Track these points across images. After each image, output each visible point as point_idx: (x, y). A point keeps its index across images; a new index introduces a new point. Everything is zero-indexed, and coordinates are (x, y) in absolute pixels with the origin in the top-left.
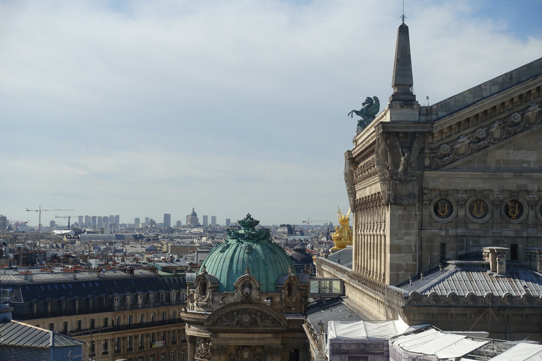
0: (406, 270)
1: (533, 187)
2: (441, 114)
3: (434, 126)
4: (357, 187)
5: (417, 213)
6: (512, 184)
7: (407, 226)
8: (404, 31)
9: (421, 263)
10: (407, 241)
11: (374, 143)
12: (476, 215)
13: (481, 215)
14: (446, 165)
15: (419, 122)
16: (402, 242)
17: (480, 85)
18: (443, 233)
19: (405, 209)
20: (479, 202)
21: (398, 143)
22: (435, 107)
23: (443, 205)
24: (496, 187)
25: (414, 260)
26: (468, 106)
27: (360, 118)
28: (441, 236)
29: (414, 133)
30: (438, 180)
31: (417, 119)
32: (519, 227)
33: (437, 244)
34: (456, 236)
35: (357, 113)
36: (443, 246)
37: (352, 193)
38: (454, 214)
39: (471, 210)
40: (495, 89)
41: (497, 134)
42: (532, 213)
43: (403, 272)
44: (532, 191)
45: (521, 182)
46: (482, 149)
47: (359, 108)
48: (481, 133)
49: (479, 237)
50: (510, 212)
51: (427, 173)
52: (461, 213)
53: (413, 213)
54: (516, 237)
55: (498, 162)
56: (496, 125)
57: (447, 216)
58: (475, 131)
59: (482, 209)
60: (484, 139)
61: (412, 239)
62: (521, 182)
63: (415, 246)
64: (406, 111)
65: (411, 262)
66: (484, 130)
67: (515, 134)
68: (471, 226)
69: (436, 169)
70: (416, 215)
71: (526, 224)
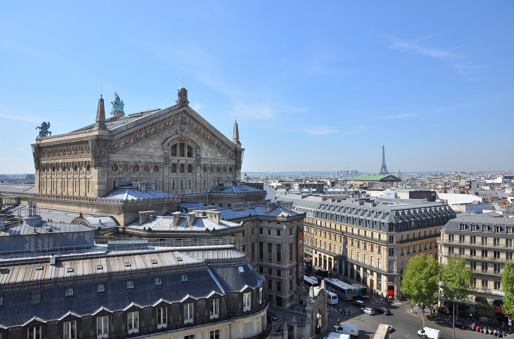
1: (143, 160)
4: (41, 159)
6: (137, 159)
7: (104, 175)
16: (102, 181)
20: (126, 166)
23: (115, 167)
24: (132, 160)
26: (124, 131)
30: (114, 157)
33: (113, 181)
35: (39, 128)
40: (132, 126)
42: (142, 170)
45: (139, 159)
47: (40, 126)
48: (128, 141)
51: (111, 155)
52: (121, 169)
57: (116, 170)
61: (105, 179)
62: (139, 159)
68: (123, 174)
71: (140, 174)
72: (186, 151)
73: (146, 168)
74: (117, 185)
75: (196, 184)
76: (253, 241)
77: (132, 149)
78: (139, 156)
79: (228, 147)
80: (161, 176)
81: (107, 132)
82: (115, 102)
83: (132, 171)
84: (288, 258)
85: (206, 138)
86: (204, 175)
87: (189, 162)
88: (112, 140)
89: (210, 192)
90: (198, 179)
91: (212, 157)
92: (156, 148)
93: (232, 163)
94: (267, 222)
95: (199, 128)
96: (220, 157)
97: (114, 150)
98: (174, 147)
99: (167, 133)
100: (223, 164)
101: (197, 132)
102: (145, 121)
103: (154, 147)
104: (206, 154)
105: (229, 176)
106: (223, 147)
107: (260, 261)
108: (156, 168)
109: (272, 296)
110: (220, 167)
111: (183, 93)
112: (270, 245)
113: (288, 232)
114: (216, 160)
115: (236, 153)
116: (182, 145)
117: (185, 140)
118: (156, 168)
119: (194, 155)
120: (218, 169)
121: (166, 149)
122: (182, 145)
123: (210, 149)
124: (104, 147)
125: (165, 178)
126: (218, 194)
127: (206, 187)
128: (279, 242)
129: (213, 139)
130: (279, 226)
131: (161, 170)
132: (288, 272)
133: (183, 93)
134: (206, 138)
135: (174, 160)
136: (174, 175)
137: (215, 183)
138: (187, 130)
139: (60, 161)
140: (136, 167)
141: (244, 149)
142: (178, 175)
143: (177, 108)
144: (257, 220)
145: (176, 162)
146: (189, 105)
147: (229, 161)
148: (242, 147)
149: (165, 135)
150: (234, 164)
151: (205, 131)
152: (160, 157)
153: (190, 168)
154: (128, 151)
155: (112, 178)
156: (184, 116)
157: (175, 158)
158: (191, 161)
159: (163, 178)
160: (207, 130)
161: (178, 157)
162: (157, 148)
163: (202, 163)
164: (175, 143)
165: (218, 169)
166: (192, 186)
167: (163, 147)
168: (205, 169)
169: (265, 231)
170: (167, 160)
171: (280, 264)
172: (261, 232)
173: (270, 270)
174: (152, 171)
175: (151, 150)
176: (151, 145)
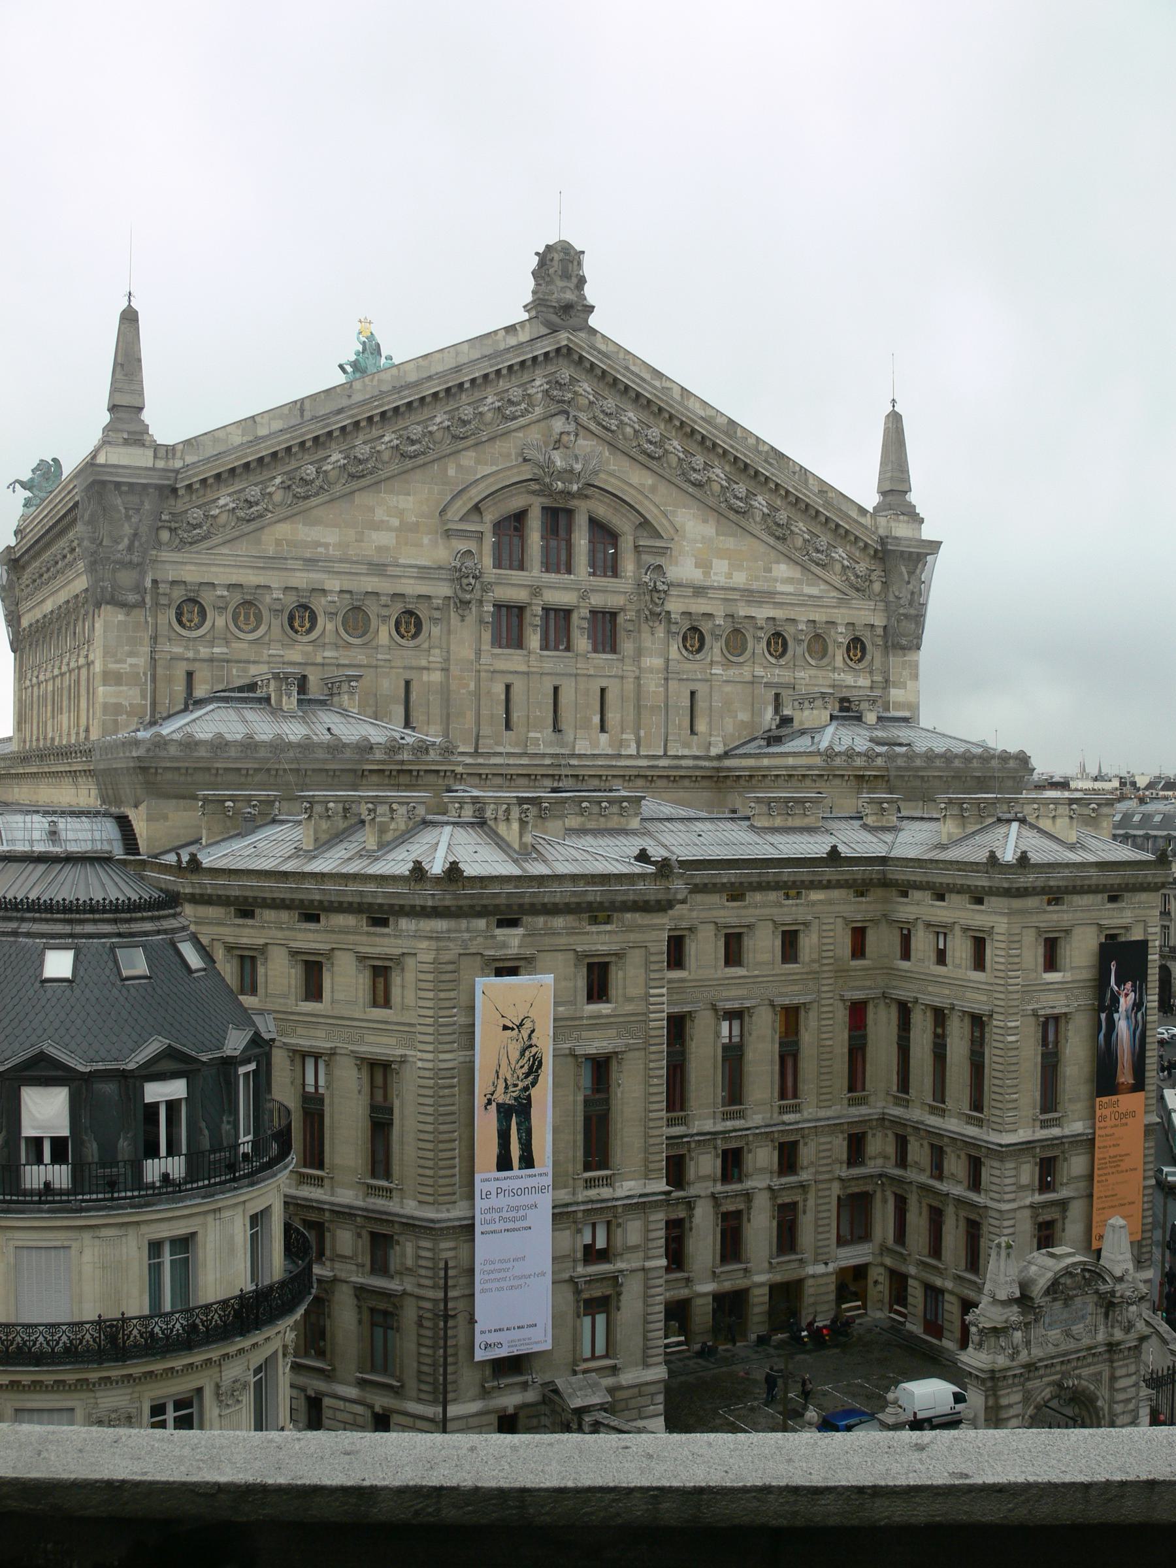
0: (129, 714)
1: (333, 584)
2: (190, 459)
3: (180, 476)
4: (23, 607)
5: (149, 619)
6: (302, 579)
8: (129, 318)
9: (154, 704)
10: (131, 665)
11: (76, 505)
12: (243, 626)
13: (251, 627)
14: (195, 542)
15: (153, 469)
16: (124, 667)
17: (253, 417)
18: (190, 655)
19: (128, 615)
20: (247, 607)
21: (119, 501)
22: (181, 446)
23: (191, 608)
25: (144, 697)
27: (28, 494)
28: (187, 659)
29: (145, 486)
30: (185, 568)
31: (150, 465)
32: (310, 648)
33: (180, 672)
34: (211, 660)
35: (24, 485)
36: (190, 675)
37: (13, 620)
38: (208, 624)
39: (235, 619)
40: (277, 425)
41: (278, 497)
42: (330, 626)
43: (124, 717)
44: (331, 591)
45: (313, 575)
46: (254, 519)
47: (26, 476)
48: (254, 492)
49: (249, 662)
50: (296, 625)
52: (220, 622)
53: (143, 619)
54: (305, 664)
55: (278, 543)
56: (278, 480)
57: (198, 627)
58: (243, 490)
59: (252, 618)
60: (257, 504)
61: (141, 662)
63: (145, 674)
64: (136, 451)
65: (138, 700)
66: (257, 489)
67: (307, 498)
68: (236, 645)
69: (178, 549)
70: (147, 622)
72: (581, 541)
73: (356, 617)
74: (200, 692)
75: (638, 708)
76: (859, 995)
77: (281, 533)
78: (311, 563)
79: (841, 534)
80: (436, 656)
81: (150, 453)
82: (355, 365)
83: (276, 631)
84: (1029, 1092)
85: (698, 485)
86: (688, 666)
87: (597, 600)
88: (174, 490)
89: (726, 755)
90: (653, 686)
91: (740, 579)
92: (407, 529)
93: (867, 614)
94: (925, 897)
95: (654, 433)
96: (789, 581)
97: (191, 536)
99: (468, 459)
100: (803, 615)
101: (650, 459)
102: (345, 402)
103: (395, 522)
104: (704, 565)
105: (849, 679)
106: (800, 526)
107: (898, 1102)
108: (410, 623)
109: (940, 1292)
110: (789, 631)
111: (559, 268)
112: (940, 1016)
113: (1033, 954)
114: (750, 596)
115: (886, 561)
116: (558, 519)
117: (569, 494)
118: (410, 623)
119: (628, 566)
120: (778, 642)
121: (463, 534)
122: (558, 519)
123: (729, 543)
124: (128, 518)
125: (455, 670)
126: (751, 762)
127: (701, 727)
128: (977, 1002)
129: (741, 489)
130: (978, 917)
131: (436, 631)
132: (1028, 1173)
133: (559, 268)
134: (694, 484)
135: (513, 587)
136: (513, 661)
137: (756, 713)
138: (585, 444)
139: (48, 606)
141: (935, 546)
142: (532, 660)
143: (524, 337)
144: (885, 883)
145: (519, 596)
146: (593, 321)
147: (843, 602)
148: (928, 533)
149: (460, 467)
150: (879, 621)
151: (693, 447)
152: (424, 573)
153: (606, 628)
154: (258, 542)
155: (175, 658)
156: (565, 372)
157: (516, 575)
158: (612, 594)
159: (446, 670)
160: (707, 445)
161: (535, 572)
162: (415, 528)
163: (675, 606)
164: (516, 503)
165: (778, 642)
166: (612, 717)
167: (445, 523)
168: (694, 637)
169: (922, 943)
170: (463, 576)
171: (979, 1123)
172: (906, 955)
173: (938, 1153)
174: (384, 634)
175: (386, 538)
176: (380, 514)
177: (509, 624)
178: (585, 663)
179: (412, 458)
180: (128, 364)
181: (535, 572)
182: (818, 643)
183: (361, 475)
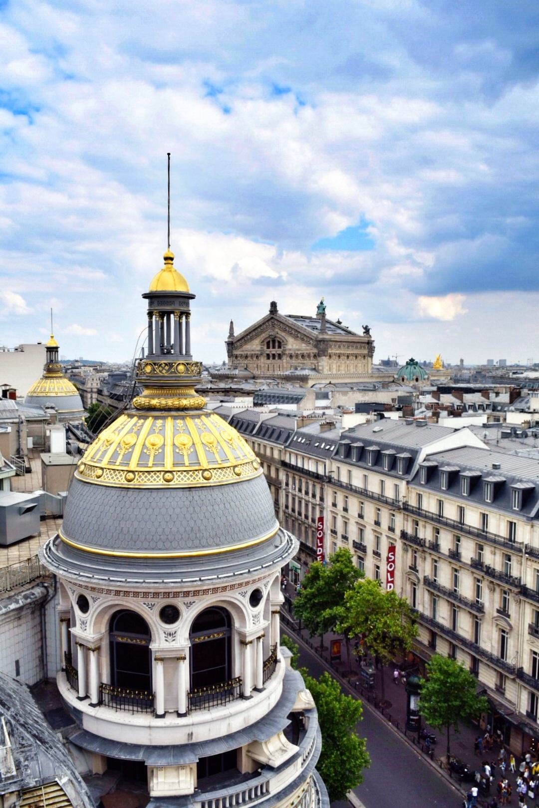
8: (232, 323)
72: (277, 344)
73: (252, 356)
98: (268, 343)
108: (257, 357)
111: (274, 305)
114: (298, 350)
118: (257, 357)
120: (303, 356)
122: (274, 341)
133: (274, 305)
136: (269, 362)
140: (246, 357)
142: (271, 361)
158: (280, 351)
161: (271, 349)
163: (287, 352)
168: (291, 357)
177: (268, 356)
178: (277, 361)
179: (257, 336)
180: (232, 328)
181: (271, 349)
182: (309, 356)
183: (252, 339)
